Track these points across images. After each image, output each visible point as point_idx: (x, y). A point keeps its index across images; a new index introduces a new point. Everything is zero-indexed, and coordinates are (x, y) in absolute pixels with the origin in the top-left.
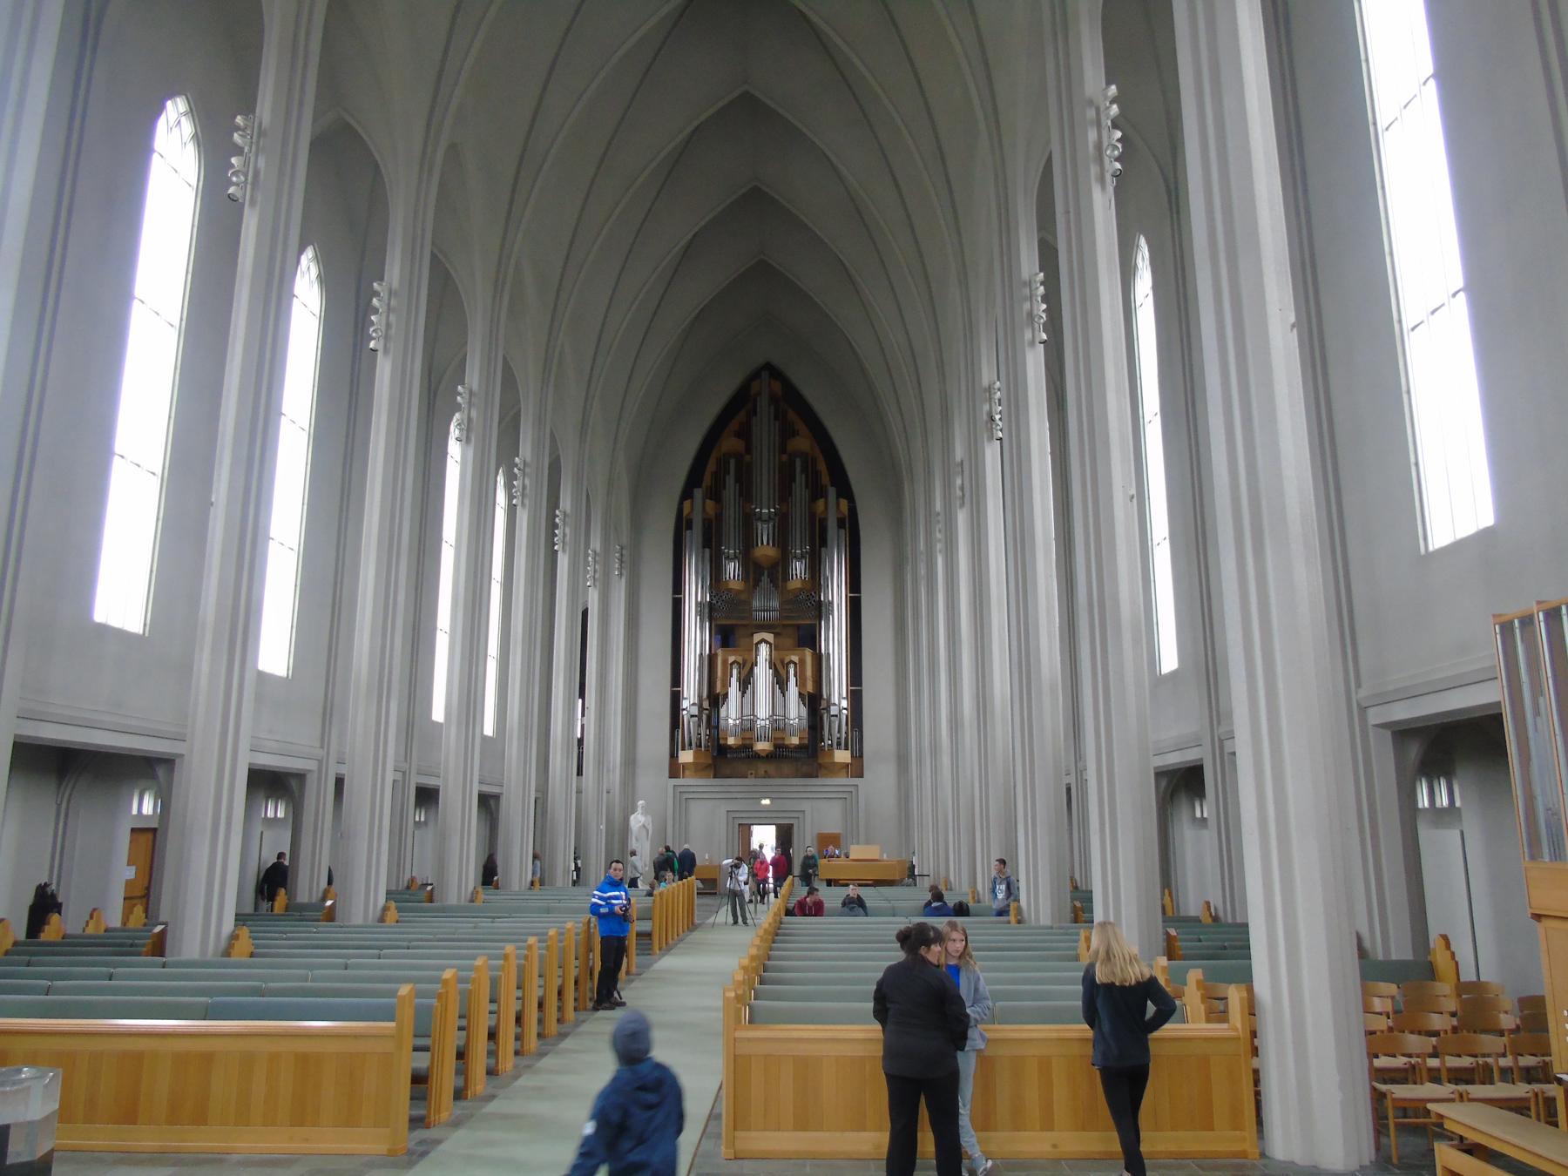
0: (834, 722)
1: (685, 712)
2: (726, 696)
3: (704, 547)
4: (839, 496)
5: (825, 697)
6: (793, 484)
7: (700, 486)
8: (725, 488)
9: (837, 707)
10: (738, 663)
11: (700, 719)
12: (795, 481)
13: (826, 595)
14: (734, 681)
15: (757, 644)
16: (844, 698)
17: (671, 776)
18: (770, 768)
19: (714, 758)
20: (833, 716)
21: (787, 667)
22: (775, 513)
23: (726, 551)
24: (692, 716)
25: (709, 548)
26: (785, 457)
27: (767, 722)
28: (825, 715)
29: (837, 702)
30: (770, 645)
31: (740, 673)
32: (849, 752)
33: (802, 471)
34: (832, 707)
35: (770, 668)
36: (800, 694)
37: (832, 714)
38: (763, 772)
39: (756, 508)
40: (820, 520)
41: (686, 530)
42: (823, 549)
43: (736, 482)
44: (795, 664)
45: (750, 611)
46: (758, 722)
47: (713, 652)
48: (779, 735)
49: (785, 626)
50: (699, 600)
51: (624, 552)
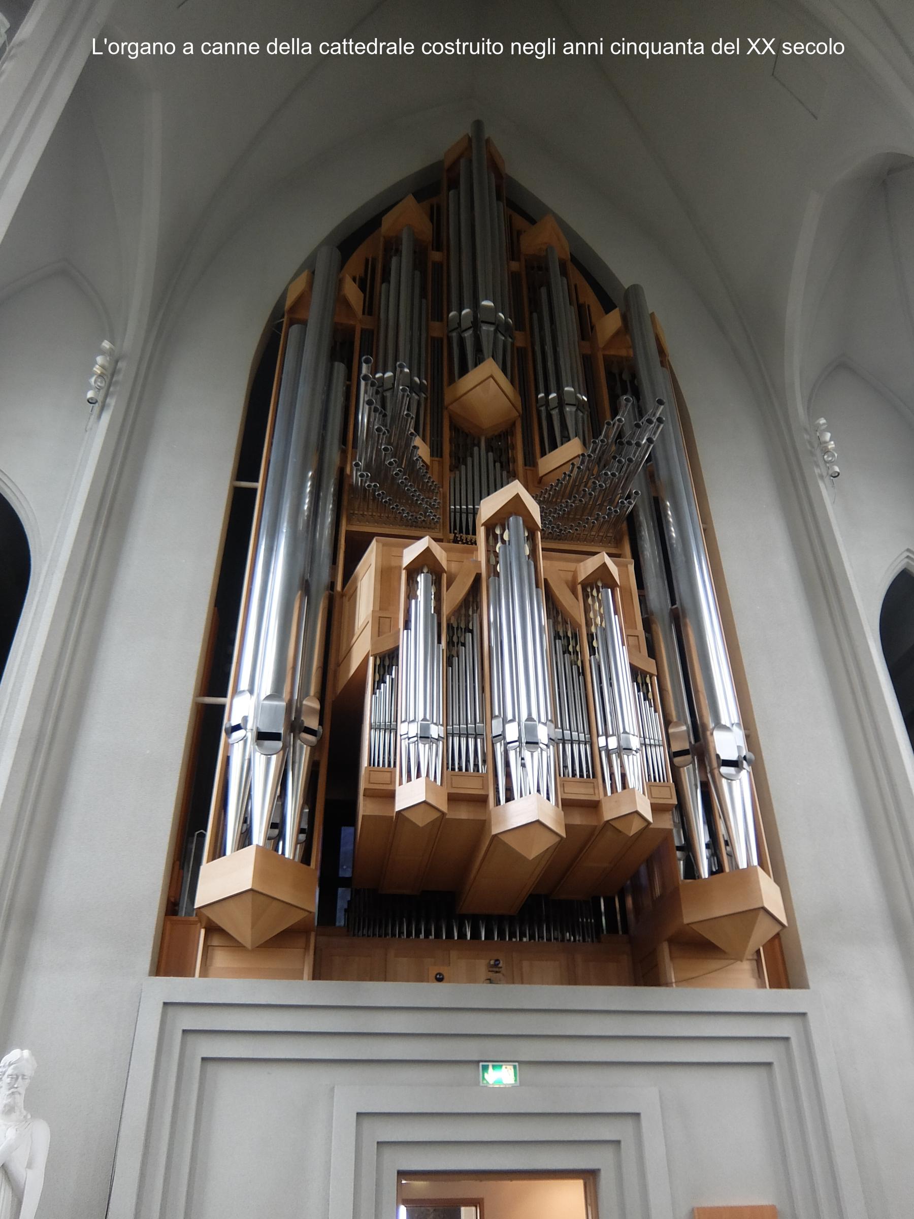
15: (490, 526)
24: (262, 736)
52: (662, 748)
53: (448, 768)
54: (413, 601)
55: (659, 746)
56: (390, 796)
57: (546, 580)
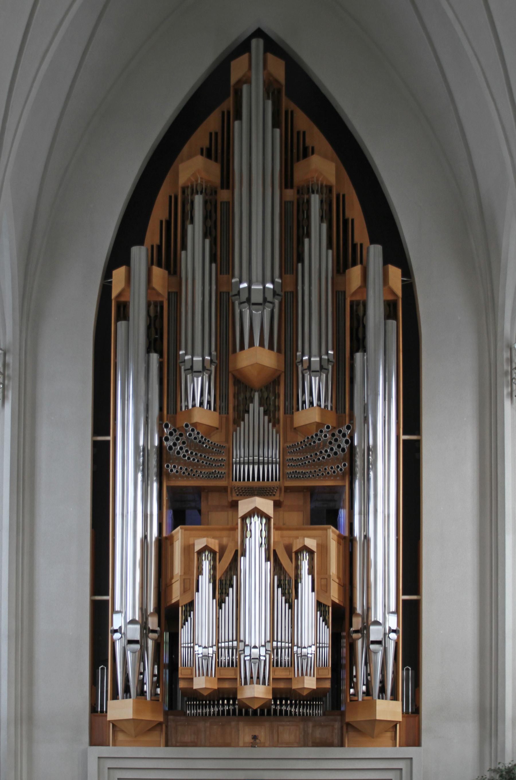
0: (376, 653)
1: (117, 636)
2: (191, 606)
3: (148, 351)
4: (387, 260)
5: (359, 610)
6: (306, 241)
7: (141, 242)
8: (184, 247)
9: (380, 628)
10: (213, 552)
11: (144, 648)
12: (309, 235)
13: (364, 436)
14: (205, 580)
15: (244, 518)
16: (393, 613)
17: (92, 743)
18: (262, 732)
19: (166, 714)
20: (374, 642)
21: (297, 559)
22: (275, 293)
23: (187, 357)
24: (130, 642)
25: (156, 352)
26: (290, 194)
27: (263, 651)
28: (359, 643)
29: (380, 619)
30: (268, 518)
31: (214, 568)
32: (400, 703)
33: (322, 220)
34: (372, 628)
35: (268, 559)
36: (320, 606)
37: (372, 638)
38: (248, 739)
39: (241, 282)
40: (352, 303)
41: (118, 319)
42: (358, 356)
43: (205, 236)
44: (311, 552)
45: (230, 465)
46: (247, 652)
47: (164, 534)
48: (281, 673)
49: (288, 490)
50: (141, 443)
51: (9, 359)
52: (328, 648)
53: (218, 666)
54: (192, 613)
55: (327, 647)
56: (191, 680)
57: (274, 551)
